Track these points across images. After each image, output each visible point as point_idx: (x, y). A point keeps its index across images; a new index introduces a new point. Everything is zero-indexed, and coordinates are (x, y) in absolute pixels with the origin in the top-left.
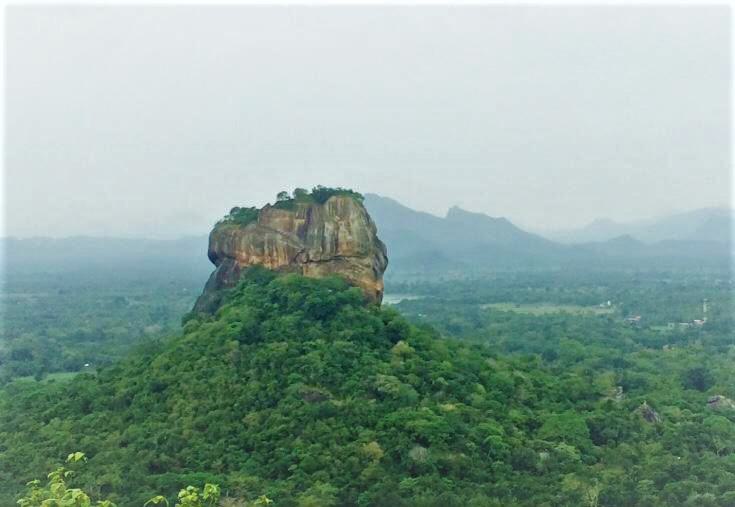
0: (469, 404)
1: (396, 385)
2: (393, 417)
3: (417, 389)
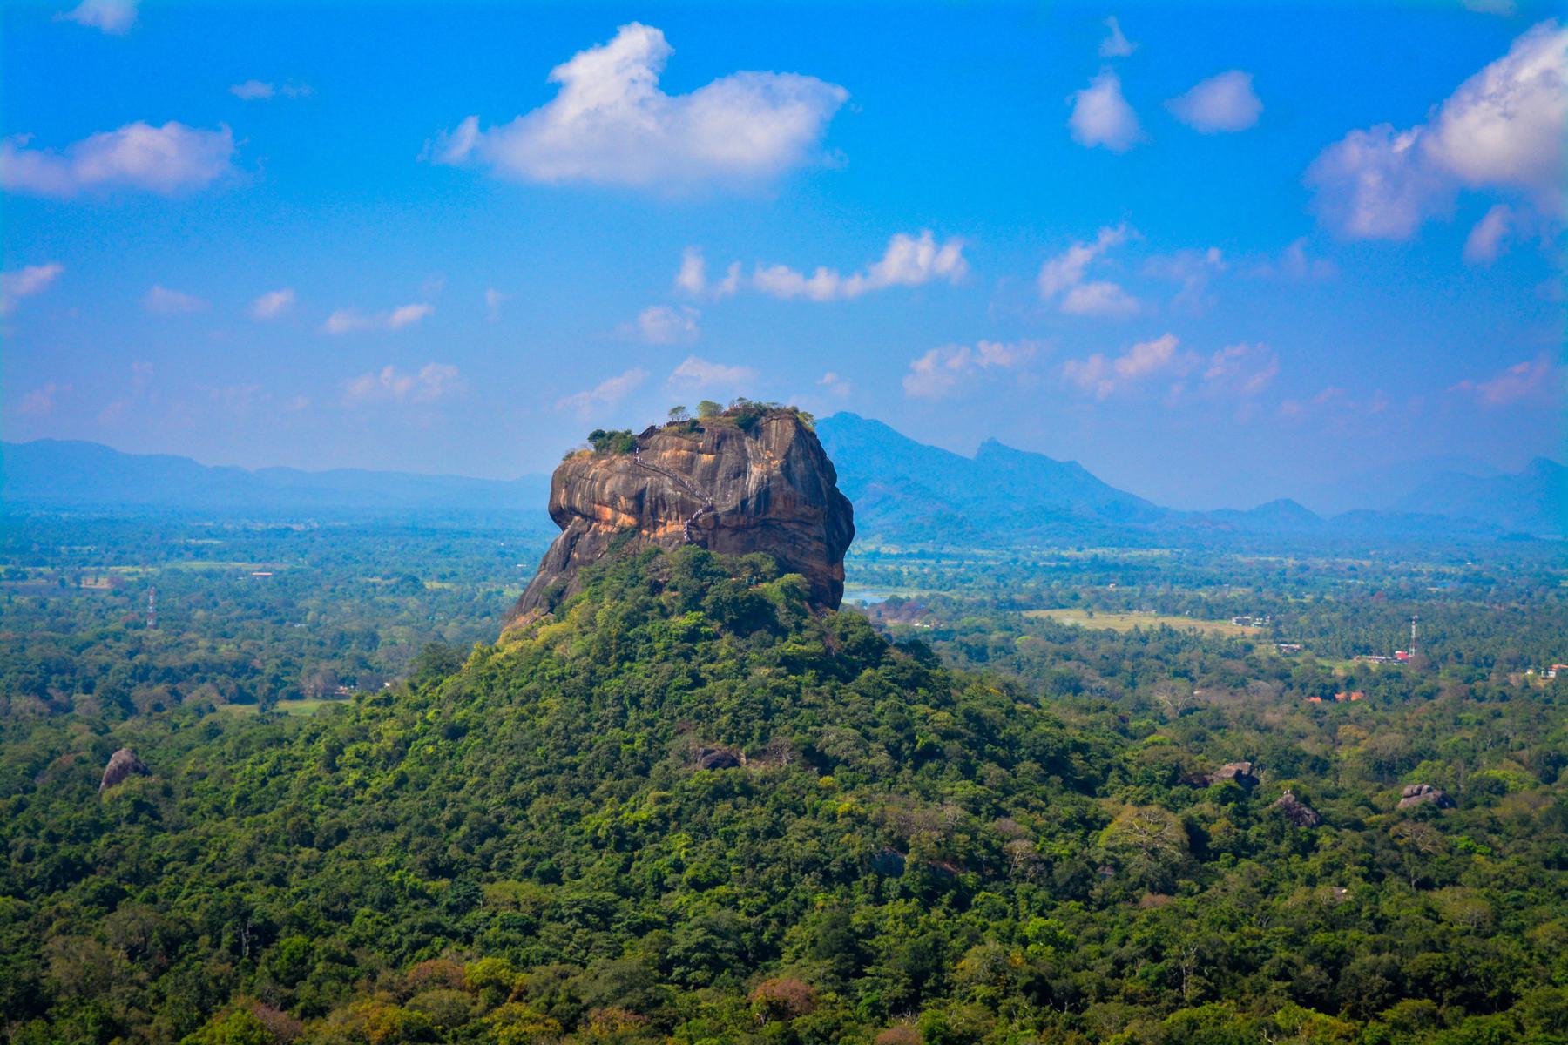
3: (895, 752)
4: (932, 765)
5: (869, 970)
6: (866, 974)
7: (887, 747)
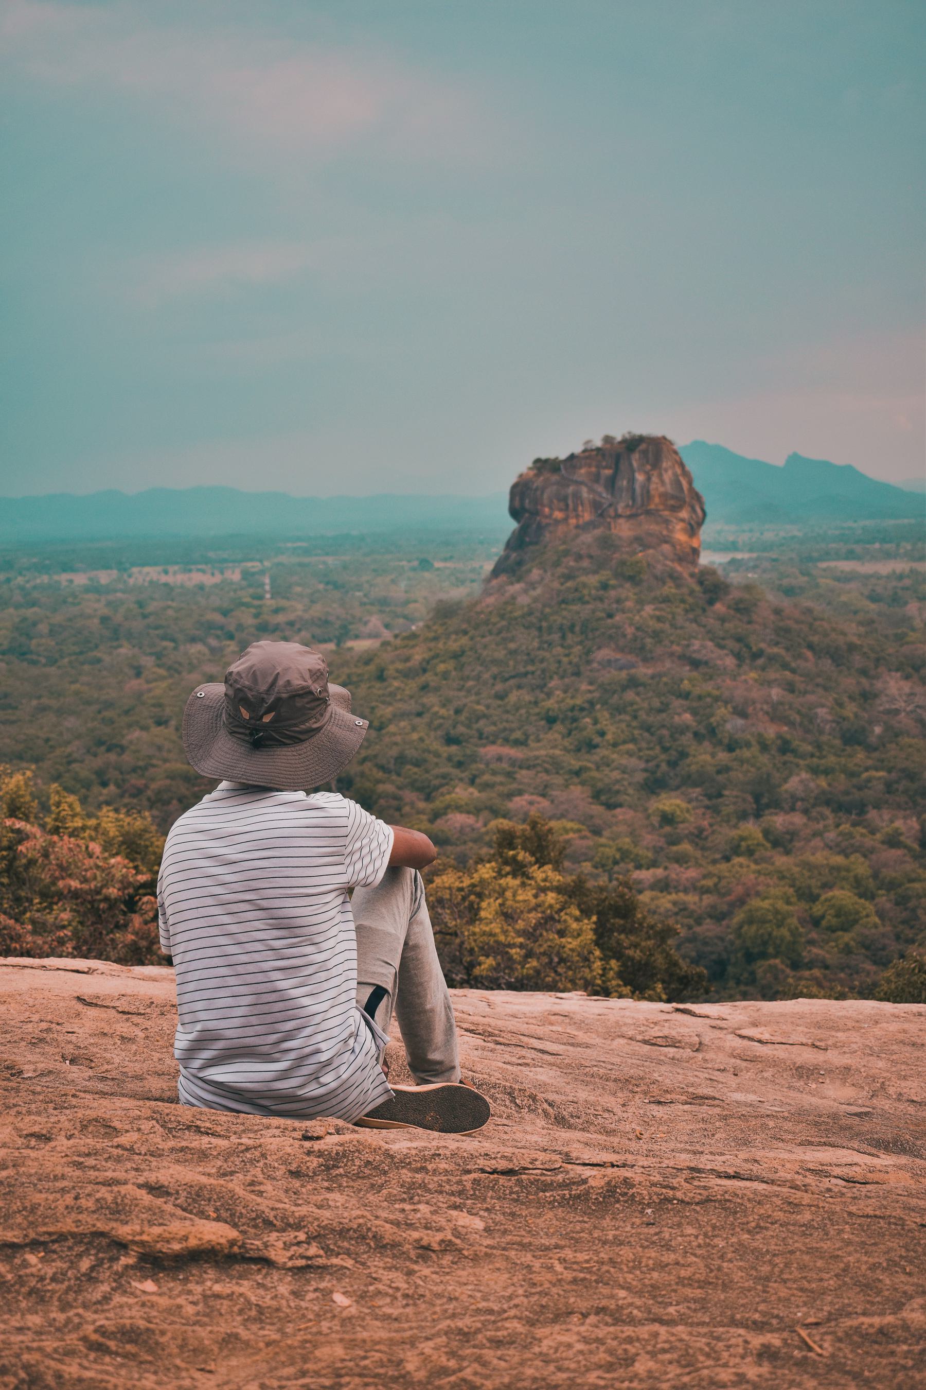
0: (793, 671)
1: (712, 652)
2: (709, 687)
3: (738, 656)
4: (760, 661)
5: (726, 793)
7: (732, 651)
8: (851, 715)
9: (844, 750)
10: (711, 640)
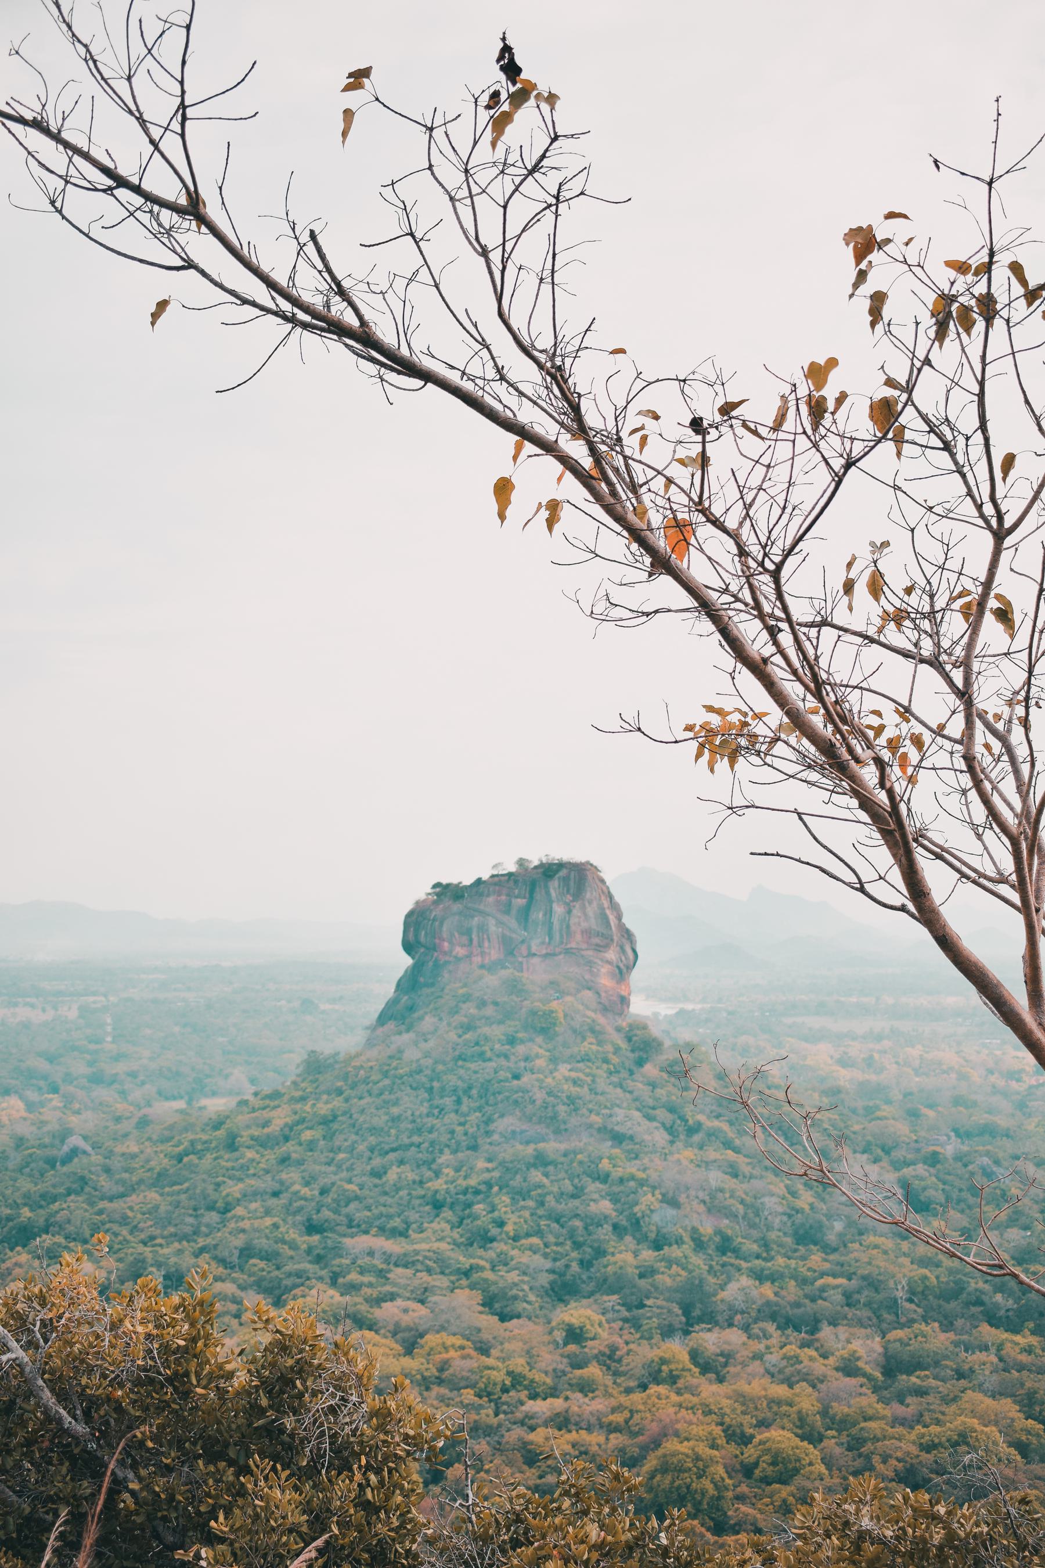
0: (737, 1150)
2: (632, 1168)
3: (670, 1130)
4: (697, 1138)
5: (649, 1302)
6: (645, 1306)
7: (663, 1124)
8: (807, 1207)
9: (796, 1250)
10: (638, 1109)
